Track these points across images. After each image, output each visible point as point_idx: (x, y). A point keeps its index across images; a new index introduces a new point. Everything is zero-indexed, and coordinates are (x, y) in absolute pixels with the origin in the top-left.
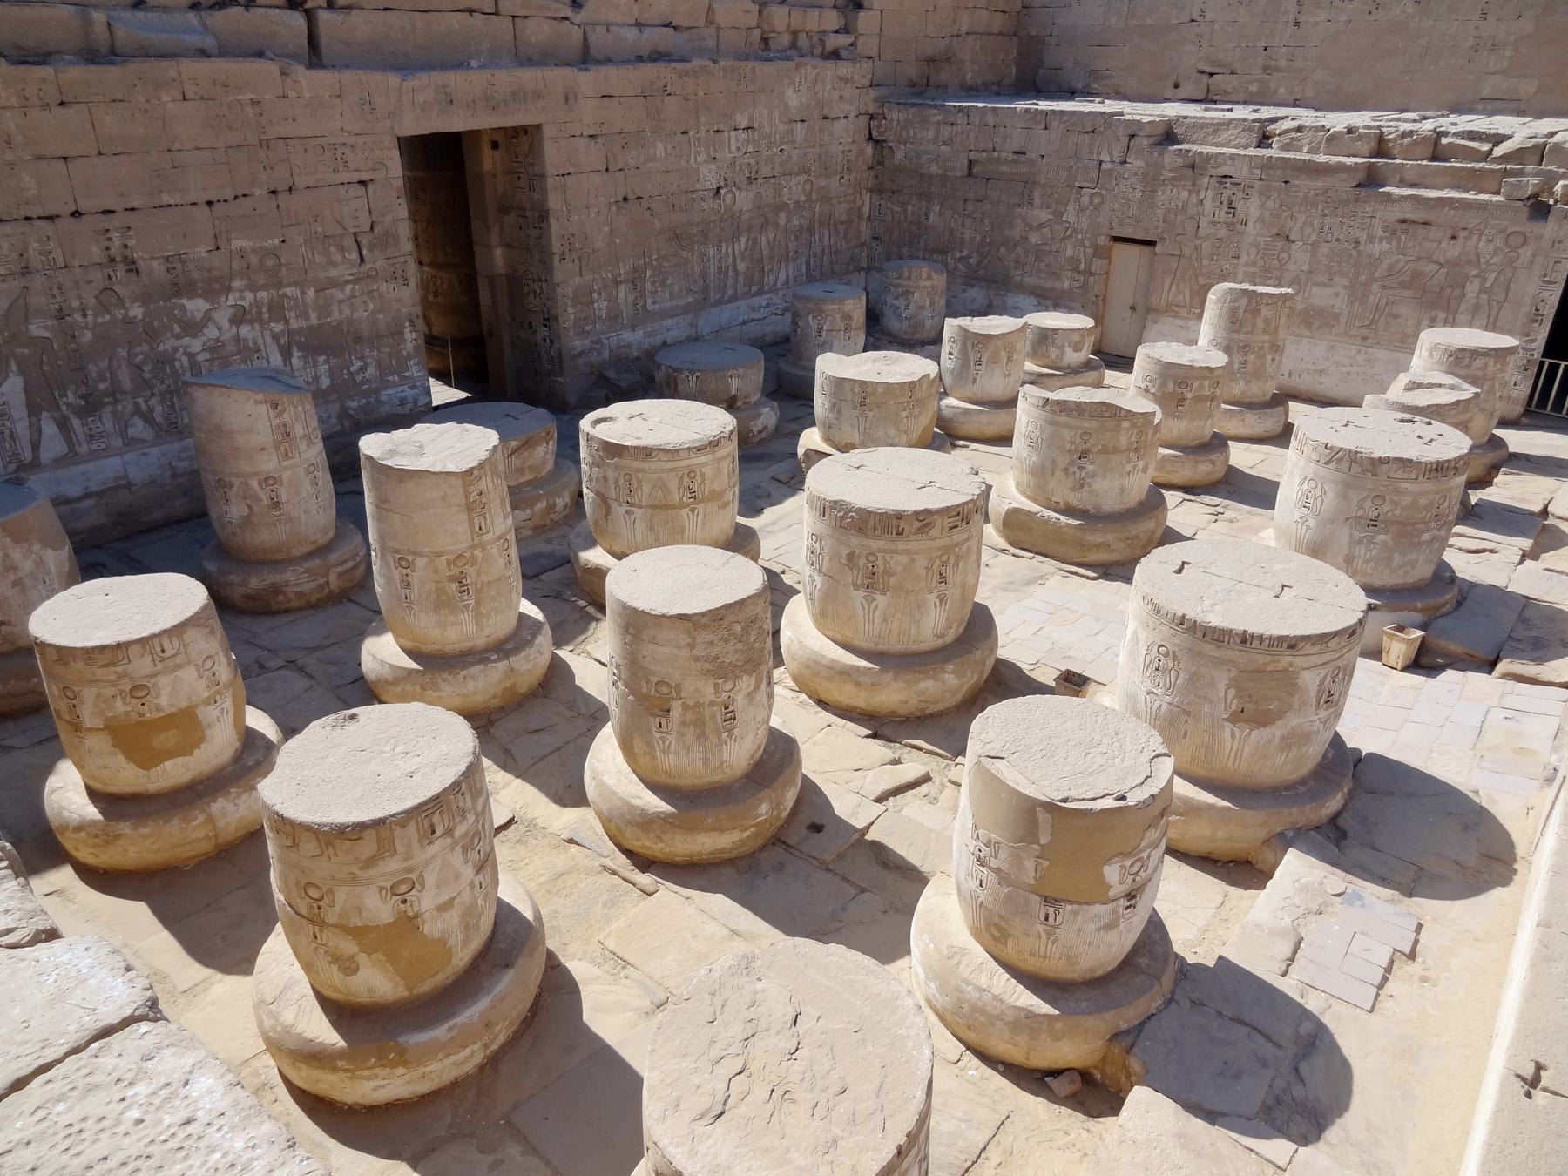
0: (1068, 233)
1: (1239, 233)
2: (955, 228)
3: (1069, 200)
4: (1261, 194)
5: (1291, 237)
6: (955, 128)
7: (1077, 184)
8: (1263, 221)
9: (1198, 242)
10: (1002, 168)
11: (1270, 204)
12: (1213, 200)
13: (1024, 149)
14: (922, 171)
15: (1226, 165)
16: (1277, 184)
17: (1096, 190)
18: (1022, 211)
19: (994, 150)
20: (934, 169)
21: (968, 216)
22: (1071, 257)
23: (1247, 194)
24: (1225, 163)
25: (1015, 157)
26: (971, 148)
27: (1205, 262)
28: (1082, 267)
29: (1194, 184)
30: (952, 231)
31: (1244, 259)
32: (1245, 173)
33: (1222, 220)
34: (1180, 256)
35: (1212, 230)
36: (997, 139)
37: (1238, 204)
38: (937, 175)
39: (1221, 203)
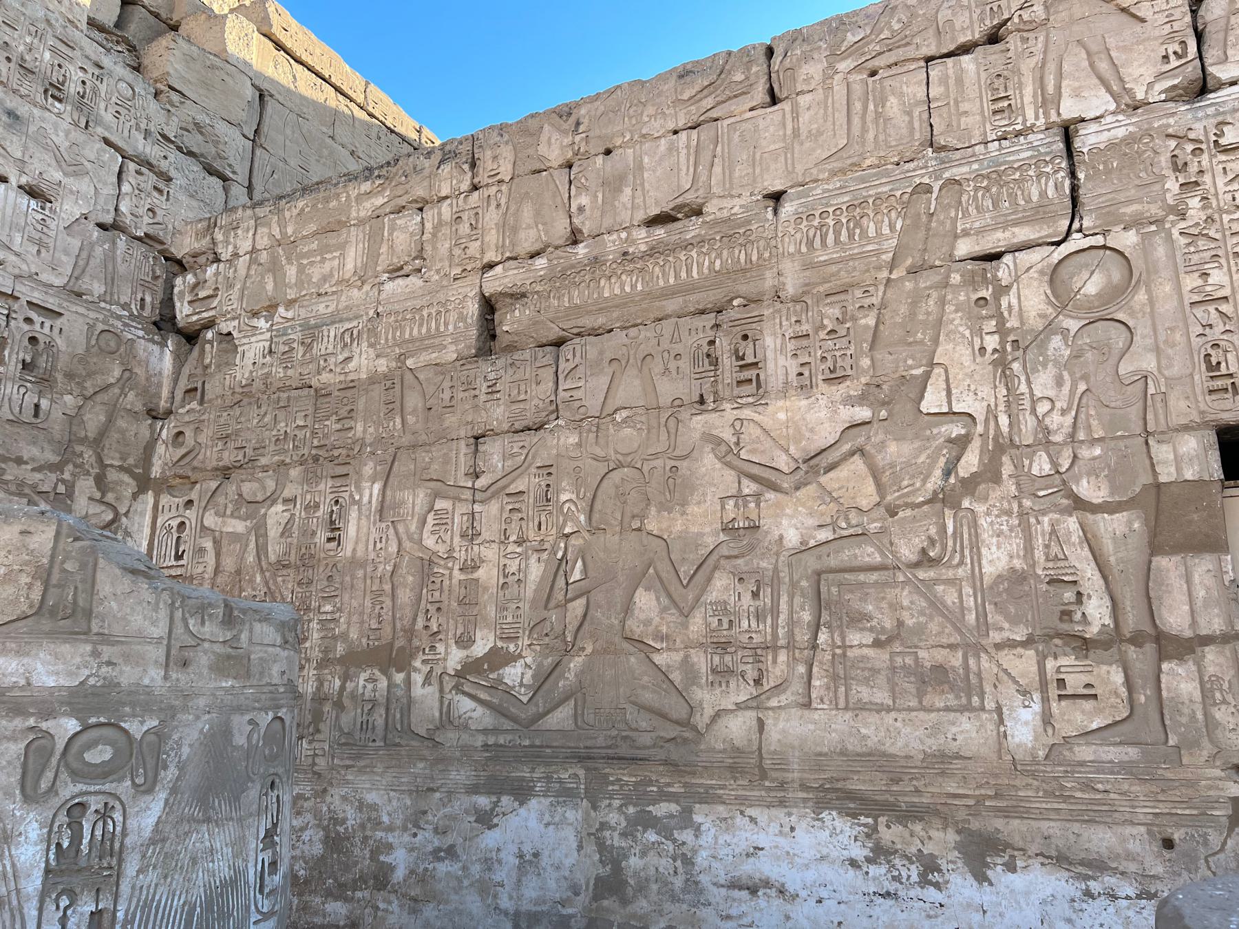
0: (971, 462)
2: (441, 549)
3: (939, 322)
6: (429, 214)
7: (964, 248)
10: (609, 289)
13: (689, 197)
14: (325, 377)
17: (1077, 242)
18: (720, 423)
19: (575, 238)
20: (364, 362)
21: (490, 492)
22: (1015, 579)
25: (660, 232)
26: (491, 256)
28: (1097, 612)
30: (427, 566)
36: (584, 200)
38: (373, 379)
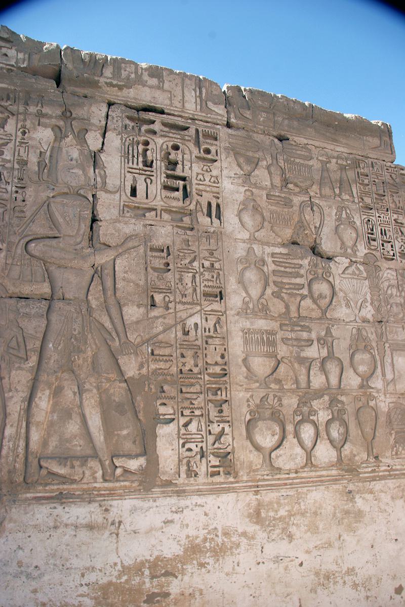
1: (208, 235)
4: (237, 154)
5: (327, 246)
8: (256, 209)
9: (103, 259)
11: (261, 175)
12: (127, 155)
15: (144, 84)
16: (267, 140)
23: (208, 151)
24: (139, 81)
27: (133, 313)
29: (67, 115)
31: (235, 300)
32: (191, 107)
33: (158, 203)
34: (50, 299)
35: (132, 227)
37: (191, 169)
39: (148, 164)
